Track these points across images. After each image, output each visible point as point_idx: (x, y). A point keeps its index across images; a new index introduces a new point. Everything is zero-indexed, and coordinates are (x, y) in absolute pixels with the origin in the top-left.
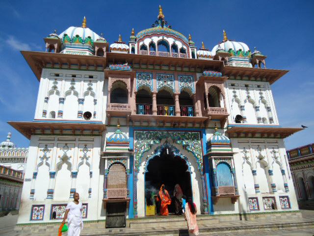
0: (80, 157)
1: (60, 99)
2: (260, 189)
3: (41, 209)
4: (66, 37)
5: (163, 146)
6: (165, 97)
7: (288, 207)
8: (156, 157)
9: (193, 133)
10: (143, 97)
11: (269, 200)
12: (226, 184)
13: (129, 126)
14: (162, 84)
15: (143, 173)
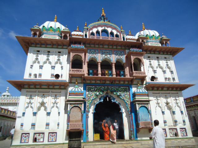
0: (52, 103)
1: (40, 66)
2: (167, 123)
3: (27, 136)
4: (44, 28)
6: (106, 65)
7: (185, 135)
8: (100, 103)
9: (124, 87)
10: (92, 65)
11: (173, 131)
12: (145, 120)
13: (83, 83)
14: (104, 57)
15: (92, 113)
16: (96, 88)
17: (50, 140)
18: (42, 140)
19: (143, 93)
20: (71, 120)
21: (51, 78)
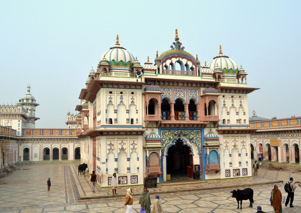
0: (131, 149)
5: (177, 139)
9: (196, 131)
11: (236, 171)
12: (214, 163)
14: (178, 97)
16: (170, 132)
17: (132, 182)
18: (126, 182)
19: (214, 137)
20: (150, 165)
21: (127, 123)
